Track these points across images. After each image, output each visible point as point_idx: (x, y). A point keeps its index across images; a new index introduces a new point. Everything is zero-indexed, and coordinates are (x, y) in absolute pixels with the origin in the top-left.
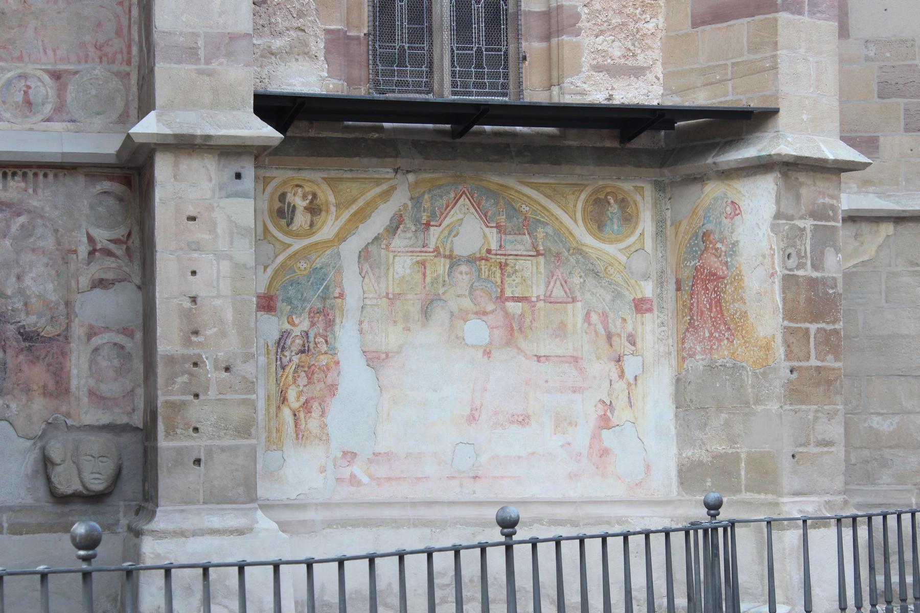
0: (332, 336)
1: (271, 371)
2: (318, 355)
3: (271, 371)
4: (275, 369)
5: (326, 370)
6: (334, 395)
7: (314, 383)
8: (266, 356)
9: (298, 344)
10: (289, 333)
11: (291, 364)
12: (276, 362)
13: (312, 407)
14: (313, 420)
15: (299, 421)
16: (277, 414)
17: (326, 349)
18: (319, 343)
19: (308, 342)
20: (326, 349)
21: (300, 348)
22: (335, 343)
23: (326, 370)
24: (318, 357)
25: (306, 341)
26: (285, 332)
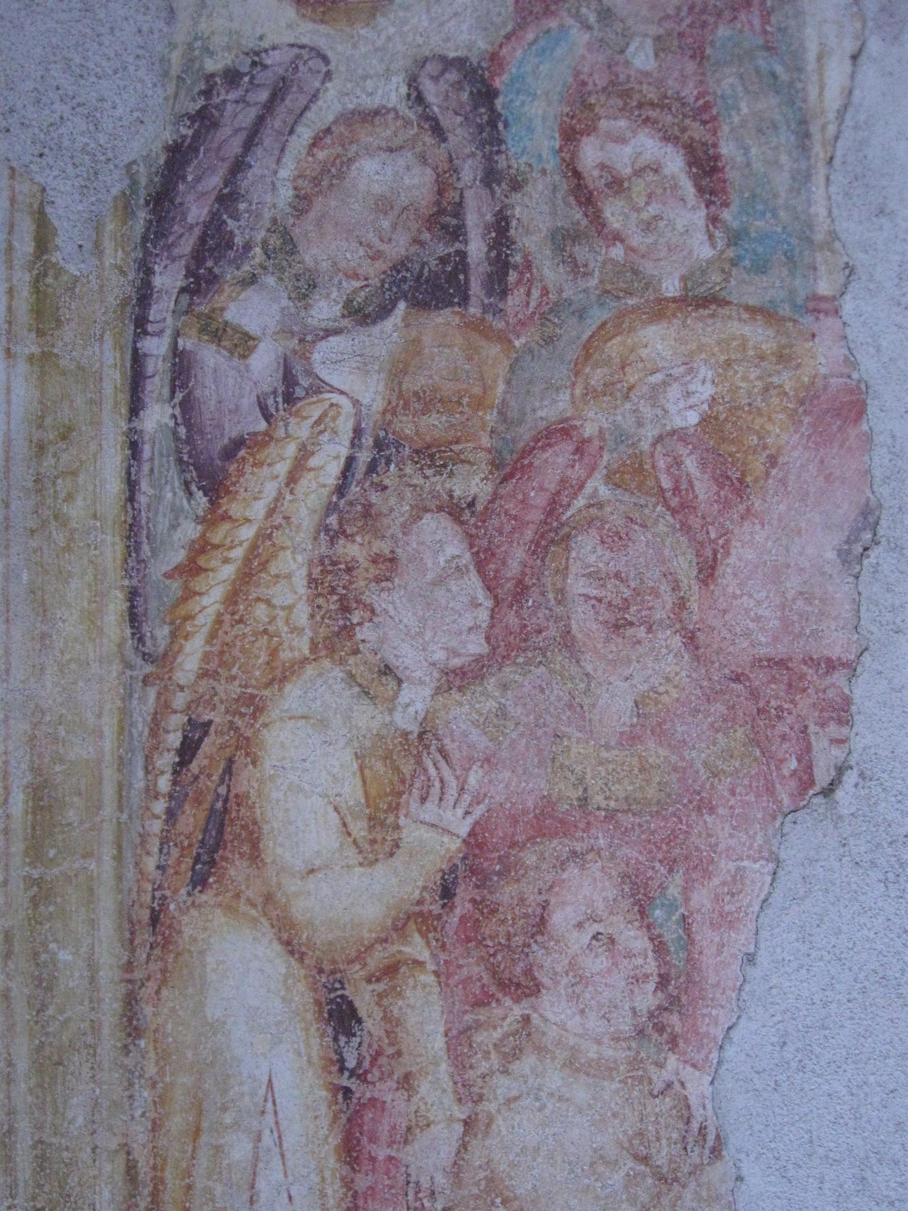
0: (769, 104)
1: (76, 511)
2: (602, 333)
3: (76, 511)
4: (114, 486)
5: (704, 489)
6: (805, 780)
7: (567, 641)
8: (30, 346)
9: (383, 205)
10: (278, 94)
11: (302, 430)
12: (135, 408)
13: (541, 924)
14: (554, 1079)
15: (386, 1091)
16: (130, 1001)
17: (706, 252)
18: (617, 185)
19: (491, 177)
20: (706, 252)
21: (399, 247)
22: (802, 179)
23: (704, 489)
24: (614, 348)
25: (469, 172)
26: (232, 77)
